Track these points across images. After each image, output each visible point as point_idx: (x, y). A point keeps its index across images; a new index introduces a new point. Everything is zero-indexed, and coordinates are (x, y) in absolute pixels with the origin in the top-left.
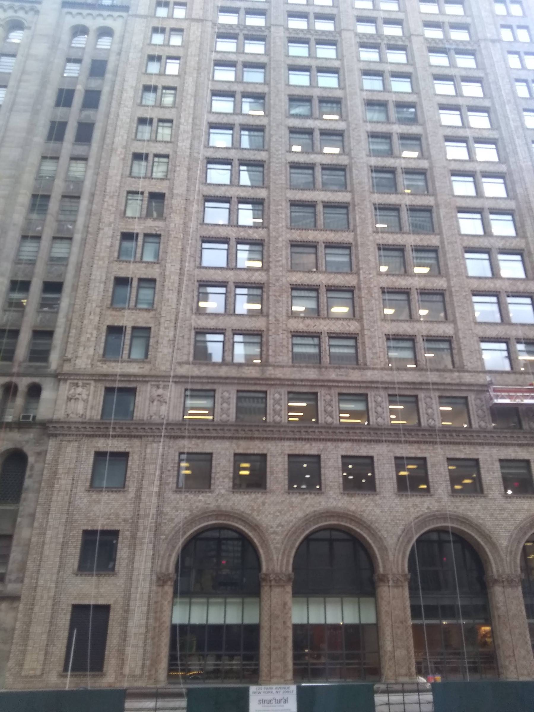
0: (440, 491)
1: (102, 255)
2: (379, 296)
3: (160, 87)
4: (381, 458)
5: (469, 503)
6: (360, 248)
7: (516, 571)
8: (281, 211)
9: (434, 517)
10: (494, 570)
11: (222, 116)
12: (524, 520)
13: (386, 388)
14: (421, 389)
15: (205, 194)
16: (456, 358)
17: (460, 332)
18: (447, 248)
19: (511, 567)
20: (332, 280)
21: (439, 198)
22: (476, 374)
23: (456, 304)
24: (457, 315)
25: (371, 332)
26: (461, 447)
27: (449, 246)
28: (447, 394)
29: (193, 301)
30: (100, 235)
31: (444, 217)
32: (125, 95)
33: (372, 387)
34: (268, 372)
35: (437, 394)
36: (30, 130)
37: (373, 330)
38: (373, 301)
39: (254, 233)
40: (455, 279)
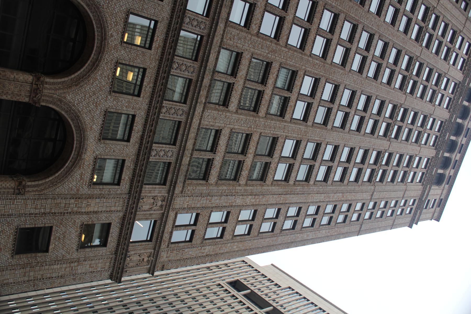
0: (123, 52)
4: (160, 8)
5: (108, 76)
6: (300, 55)
7: (43, 101)
8: (337, 3)
9: (104, 38)
10: (48, 80)
12: (85, 122)
13: (209, 35)
14: (201, 66)
16: (212, 106)
17: (230, 115)
18: (282, 123)
19: (48, 96)
20: (287, 24)
21: (311, 128)
22: (200, 117)
23: (248, 118)
24: (242, 116)
25: (249, 41)
26: (152, 85)
27: (283, 126)
28: (192, 88)
31: (300, 128)
33: (213, 23)
35: (194, 79)
37: (249, 42)
38: (267, 52)
40: (263, 123)
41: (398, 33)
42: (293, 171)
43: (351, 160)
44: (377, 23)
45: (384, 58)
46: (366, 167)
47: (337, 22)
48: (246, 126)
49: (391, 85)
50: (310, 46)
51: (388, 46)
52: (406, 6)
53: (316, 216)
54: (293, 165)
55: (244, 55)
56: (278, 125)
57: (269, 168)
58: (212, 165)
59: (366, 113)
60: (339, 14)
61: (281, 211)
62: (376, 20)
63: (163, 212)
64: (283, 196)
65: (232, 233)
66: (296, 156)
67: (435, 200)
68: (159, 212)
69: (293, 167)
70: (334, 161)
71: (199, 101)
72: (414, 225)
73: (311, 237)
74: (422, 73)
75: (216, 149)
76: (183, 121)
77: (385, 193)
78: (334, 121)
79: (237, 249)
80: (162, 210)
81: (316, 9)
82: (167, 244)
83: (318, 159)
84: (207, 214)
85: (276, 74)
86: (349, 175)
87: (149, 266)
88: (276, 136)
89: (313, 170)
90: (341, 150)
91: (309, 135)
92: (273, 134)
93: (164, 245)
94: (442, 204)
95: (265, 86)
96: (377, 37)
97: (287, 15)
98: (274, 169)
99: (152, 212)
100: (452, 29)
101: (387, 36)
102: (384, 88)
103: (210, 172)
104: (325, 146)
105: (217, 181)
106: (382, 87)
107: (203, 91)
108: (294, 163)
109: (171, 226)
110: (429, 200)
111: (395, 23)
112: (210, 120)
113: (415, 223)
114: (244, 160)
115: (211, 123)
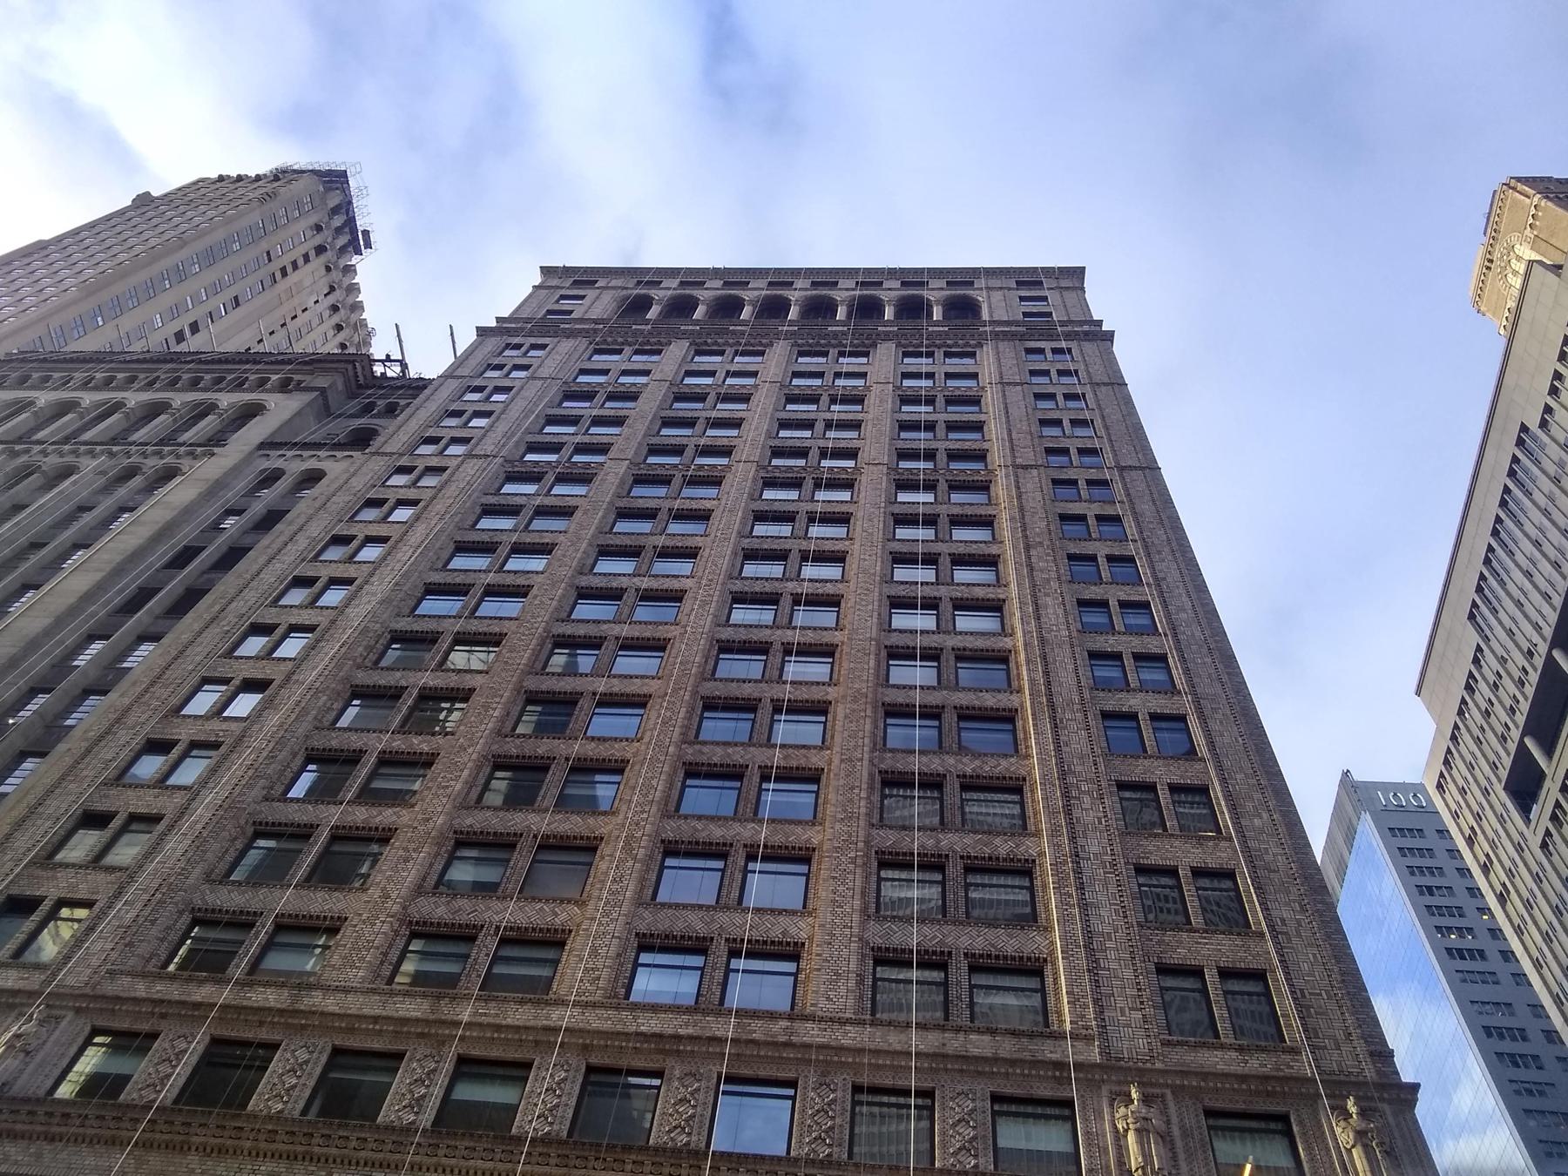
1: (85, 773)
2: (651, 857)
3: (361, 537)
8: (495, 705)
11: (456, 574)
15: (358, 682)
22: (836, 1026)
27: (843, 766)
29: (221, 859)
30: (102, 744)
32: (289, 547)
34: (306, 1000)
36: (88, 597)
38: (630, 863)
39: (425, 741)
40: (838, 826)
42: (977, 703)
43: (930, 554)
47: (548, 692)
48: (851, 877)
49: (709, 510)
50: (613, 748)
51: (607, 546)
52: (502, 530)
53: (1113, 603)
54: (961, 708)
55: (643, 929)
56: (842, 782)
57: (978, 777)
58: (989, 956)
60: (526, 691)
61: (1109, 708)
63: (1168, 1092)
64: (1058, 716)
65: (1211, 843)
66: (932, 707)
67: (1022, 299)
68: (1171, 1104)
69: (968, 708)
70: (935, 598)
71: (782, 1039)
72: (1104, 328)
73: (1185, 598)
74: (674, 442)
75: (934, 953)
76: (850, 1079)
77: (1014, 436)
78: (820, 629)
79: (1265, 815)
80: (1163, 1096)
81: (511, 757)
82: (1287, 1057)
83: (934, 645)
84: (1156, 939)
85: (694, 823)
86: (974, 546)
87: (1386, 1107)
88: (878, 778)
89: (971, 650)
90: (902, 587)
91: (864, 685)
92: (871, 788)
93: (1292, 1067)
94: (1027, 280)
95: (731, 845)
97: (530, 830)
98: (977, 763)
99: (1176, 1132)
100: (560, 404)
103: (1013, 958)
104: (895, 634)
105: (1038, 927)
107: (755, 1032)
108: (955, 707)
109: (1219, 1053)
110: (1026, 315)
112: (843, 991)
113: (1098, 328)
114: (962, 857)
115: (852, 983)
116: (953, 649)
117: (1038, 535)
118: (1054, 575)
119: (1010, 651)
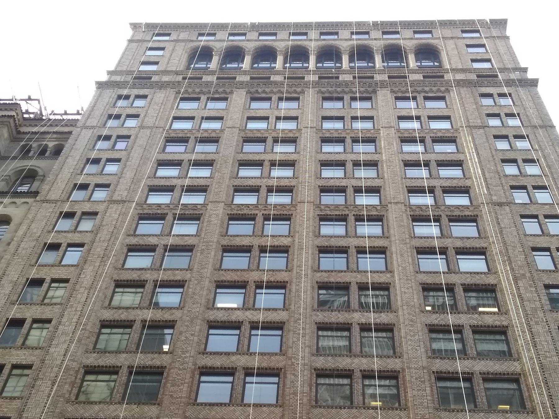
41: (195, 269)
44: (187, 326)
45: (245, 282)
46: (450, 240)
51: (222, 281)
59: (350, 283)
62: (181, 329)
96: (211, 313)
101: (205, 293)
102: (295, 260)
106: (295, 267)
111: (180, 281)
116: (480, 373)
117: (520, 267)
118: (538, 304)
119: (520, 374)
